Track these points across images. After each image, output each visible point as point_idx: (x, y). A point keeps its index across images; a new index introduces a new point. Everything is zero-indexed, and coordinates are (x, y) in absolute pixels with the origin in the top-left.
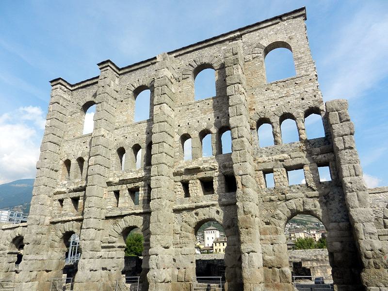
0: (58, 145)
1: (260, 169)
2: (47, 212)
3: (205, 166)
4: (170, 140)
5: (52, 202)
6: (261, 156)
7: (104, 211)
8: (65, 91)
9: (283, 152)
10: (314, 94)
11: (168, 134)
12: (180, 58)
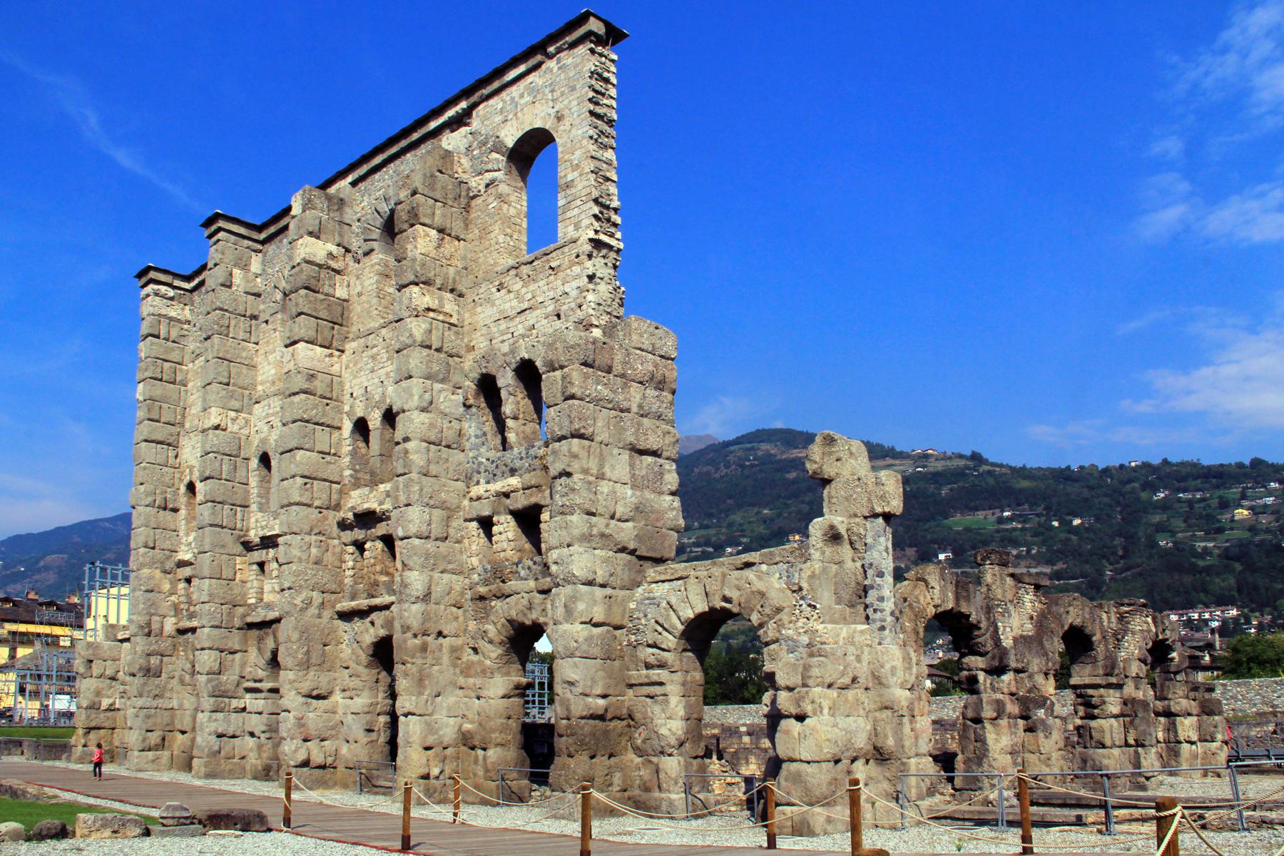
0: (169, 445)
1: (470, 516)
2: (165, 607)
3: (385, 507)
4: (323, 439)
5: (173, 584)
6: (478, 483)
7: (241, 610)
8: (172, 299)
9: (513, 472)
10: (579, 301)
11: (317, 424)
12: (362, 186)
